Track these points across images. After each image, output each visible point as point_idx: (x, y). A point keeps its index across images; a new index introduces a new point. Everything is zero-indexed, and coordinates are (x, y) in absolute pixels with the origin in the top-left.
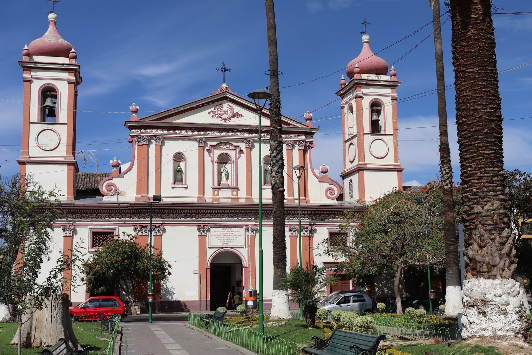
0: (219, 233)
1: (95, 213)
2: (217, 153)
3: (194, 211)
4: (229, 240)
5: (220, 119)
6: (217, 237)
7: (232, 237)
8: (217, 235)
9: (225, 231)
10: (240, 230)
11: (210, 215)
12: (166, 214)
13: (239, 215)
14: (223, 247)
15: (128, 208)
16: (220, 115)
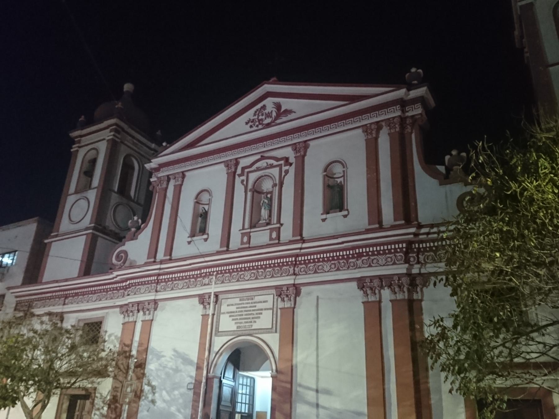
0: (233, 308)
1: (86, 294)
2: (253, 177)
3: (199, 272)
4: (249, 320)
5: (260, 127)
6: (230, 316)
7: (254, 312)
8: (231, 312)
9: (244, 302)
10: (269, 298)
11: (223, 276)
12: (162, 284)
13: (268, 270)
14: (240, 333)
15: (115, 279)
16: (261, 122)
